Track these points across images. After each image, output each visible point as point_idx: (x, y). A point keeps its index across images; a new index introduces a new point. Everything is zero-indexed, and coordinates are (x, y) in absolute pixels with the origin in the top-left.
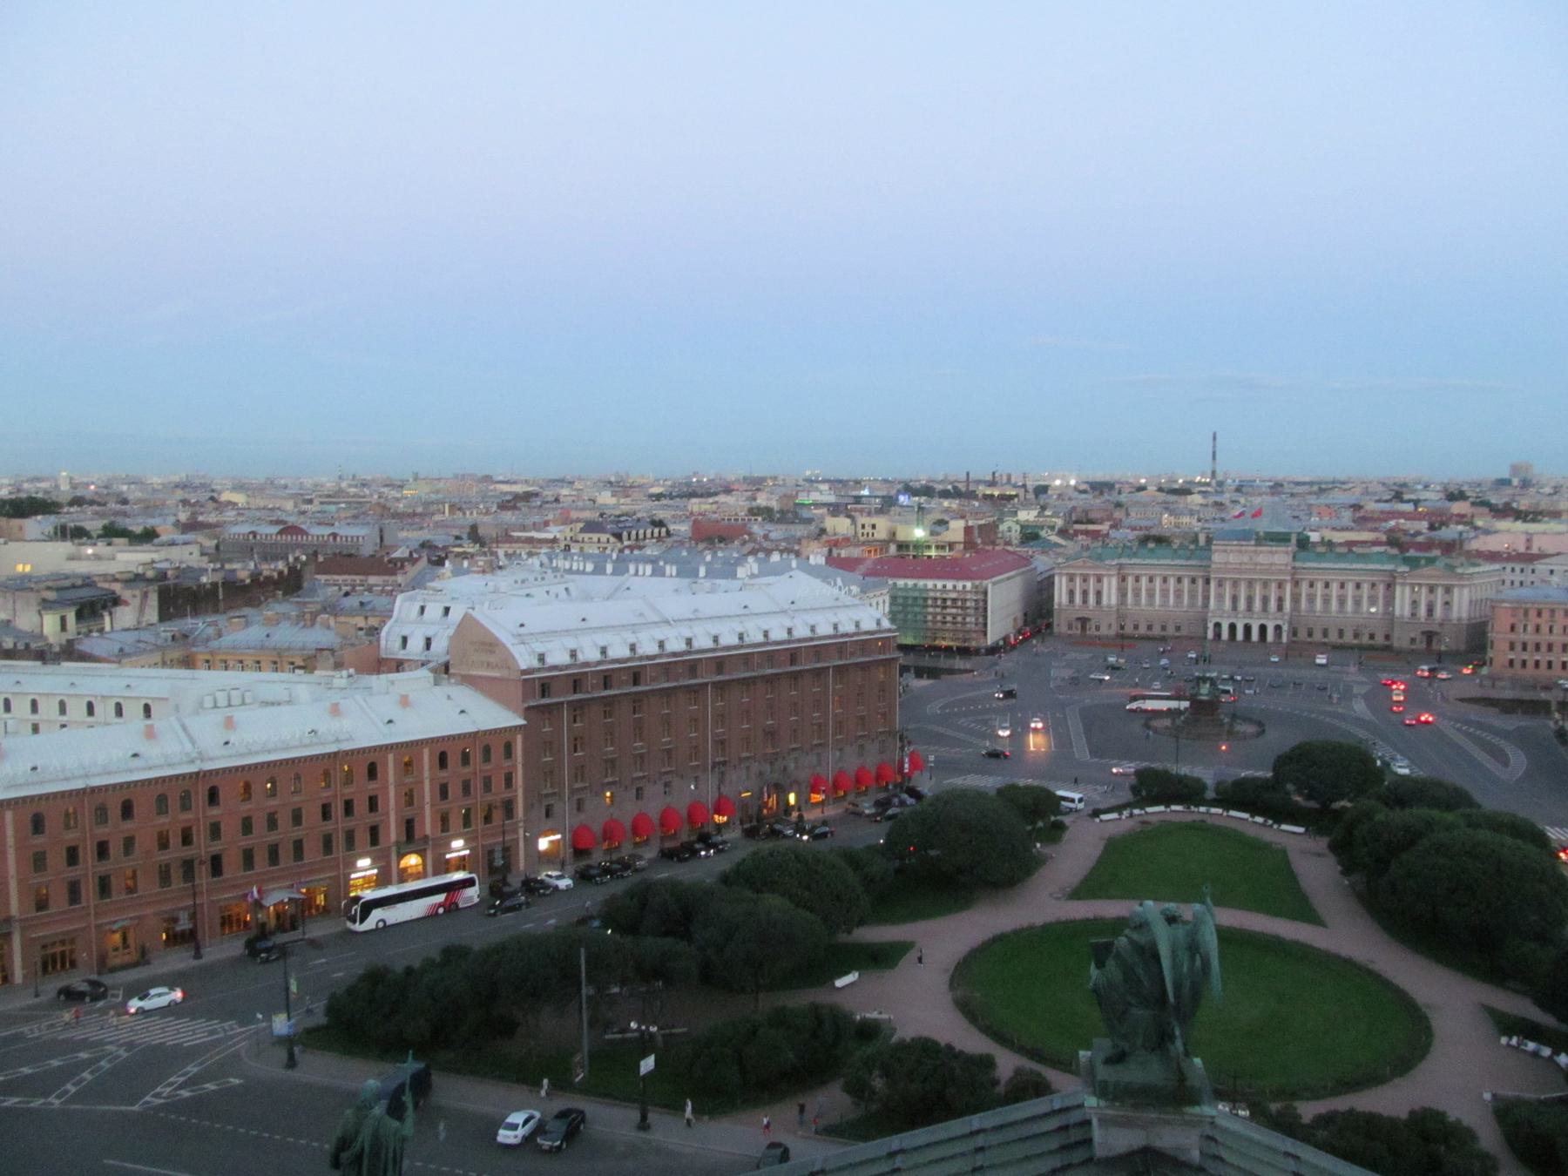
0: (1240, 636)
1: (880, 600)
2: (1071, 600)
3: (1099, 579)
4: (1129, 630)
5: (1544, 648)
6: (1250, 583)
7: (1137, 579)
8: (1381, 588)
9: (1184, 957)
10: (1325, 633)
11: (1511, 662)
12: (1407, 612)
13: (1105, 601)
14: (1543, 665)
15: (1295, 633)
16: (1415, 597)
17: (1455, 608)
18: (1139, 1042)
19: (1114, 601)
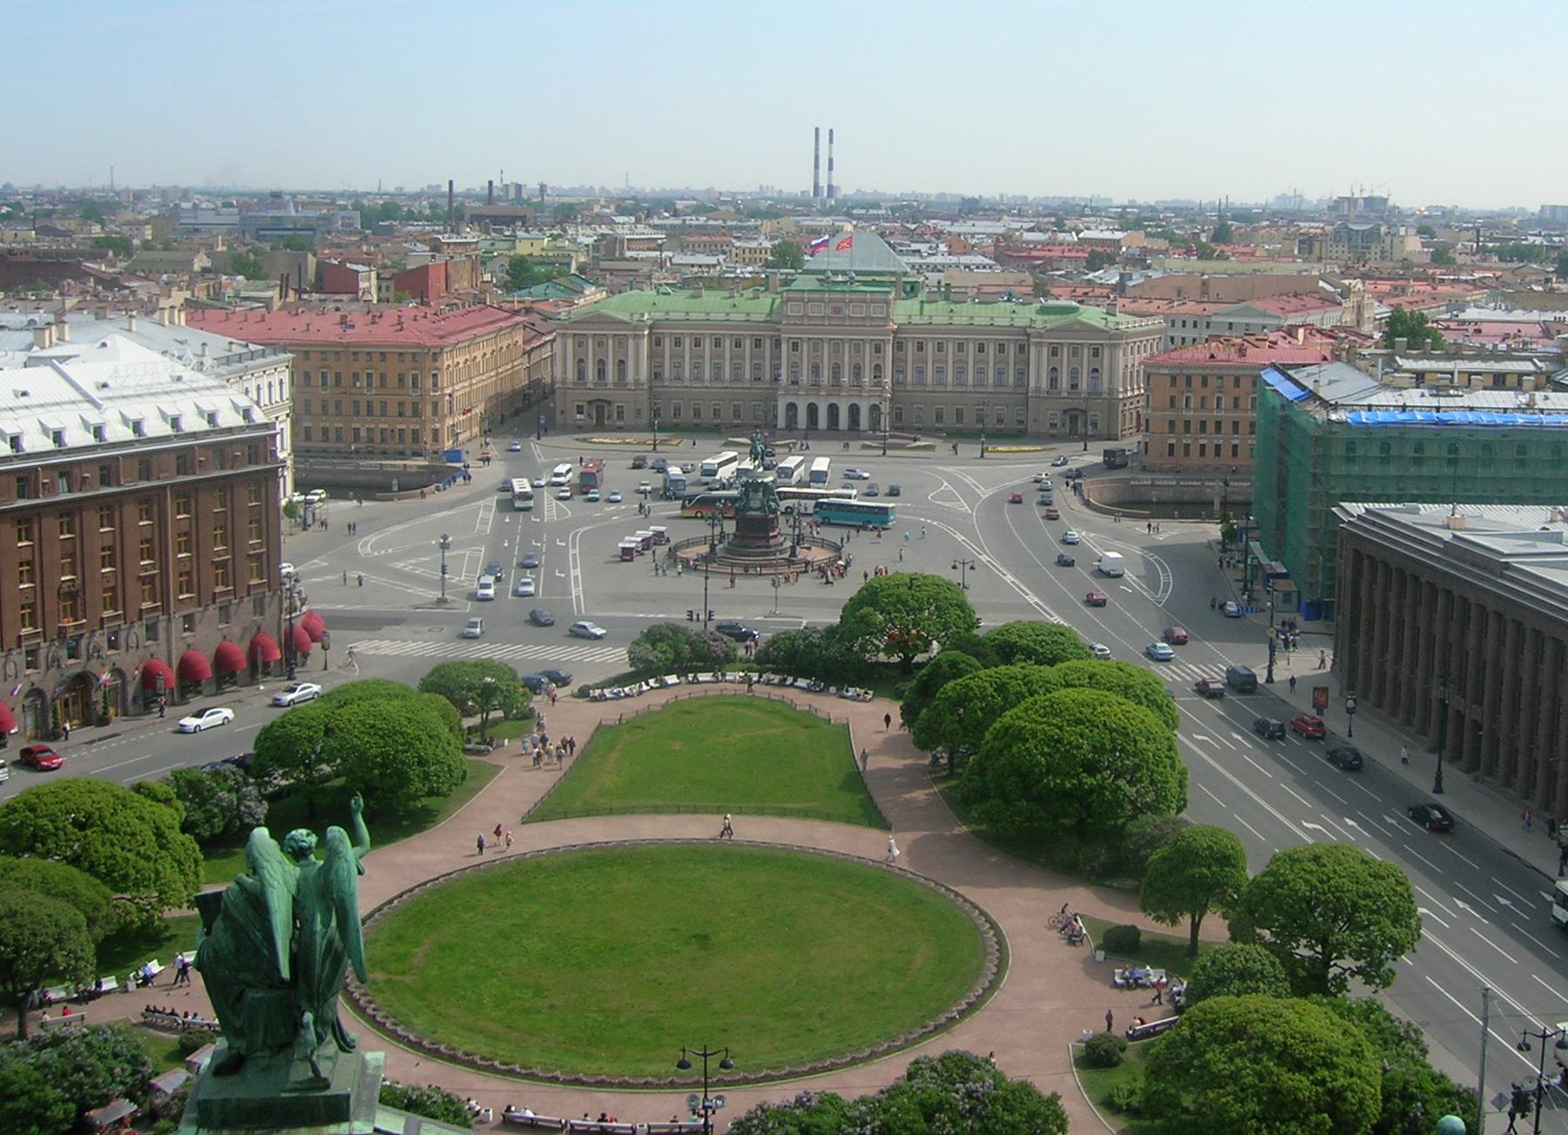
0: (823, 422)
5: (1211, 427)
6: (837, 345)
7: (678, 342)
8: (1011, 350)
11: (1171, 446)
12: (1045, 384)
13: (630, 376)
14: (1210, 451)
16: (1055, 362)
17: (1105, 378)
18: (261, 1035)
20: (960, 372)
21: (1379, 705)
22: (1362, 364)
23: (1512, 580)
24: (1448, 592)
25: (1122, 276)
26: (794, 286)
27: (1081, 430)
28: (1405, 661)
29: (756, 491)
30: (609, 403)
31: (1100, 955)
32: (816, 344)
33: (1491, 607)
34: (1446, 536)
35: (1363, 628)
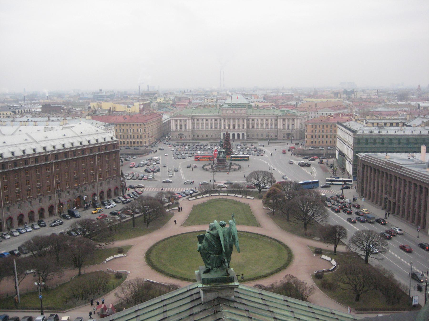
1: (112, 131)
2: (177, 128)
3: (185, 121)
4: (196, 137)
5: (321, 137)
7: (198, 120)
8: (274, 120)
9: (227, 237)
10: (257, 135)
11: (312, 141)
12: (282, 128)
13: (187, 128)
14: (321, 142)
15: (248, 136)
16: (284, 123)
17: (296, 126)
19: (190, 128)
20: (262, 125)
21: (369, 199)
22: (358, 121)
23: (403, 170)
24: (387, 173)
25: (296, 103)
26: (224, 106)
27: (290, 138)
28: (376, 189)
29: (221, 153)
30: (183, 134)
31: (314, 255)
32: (229, 120)
33: (398, 176)
34: (386, 160)
35: (365, 181)
